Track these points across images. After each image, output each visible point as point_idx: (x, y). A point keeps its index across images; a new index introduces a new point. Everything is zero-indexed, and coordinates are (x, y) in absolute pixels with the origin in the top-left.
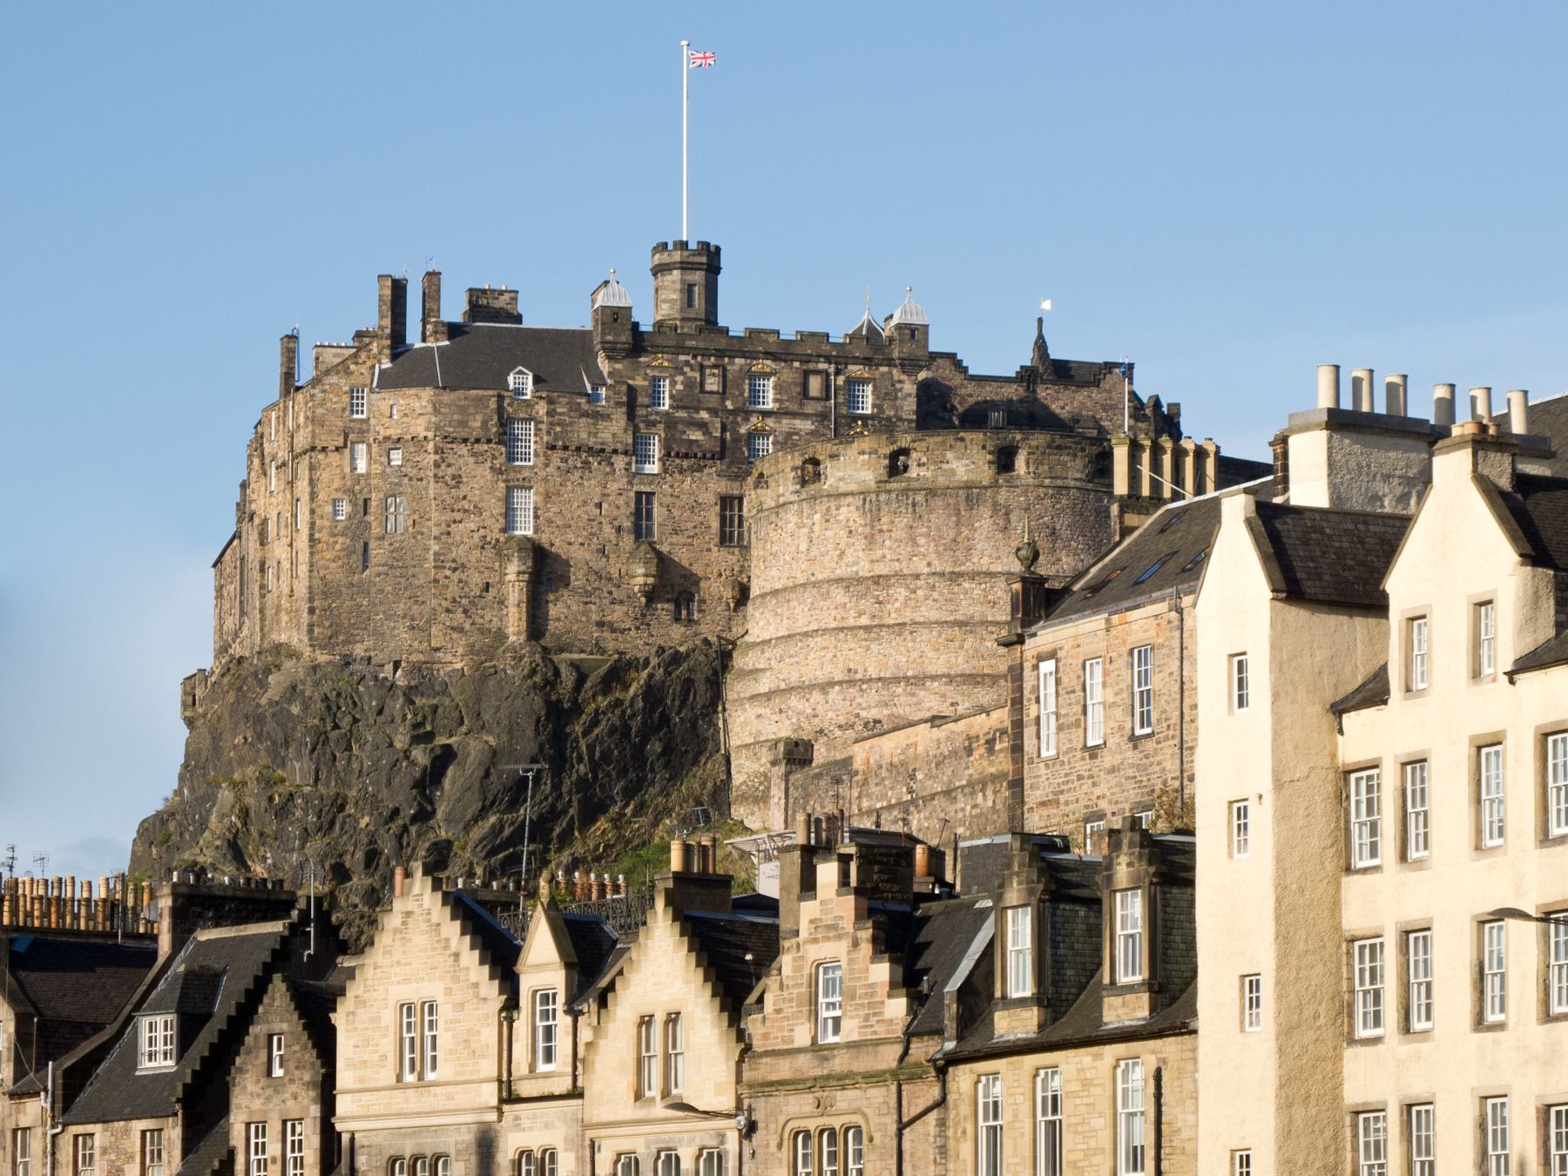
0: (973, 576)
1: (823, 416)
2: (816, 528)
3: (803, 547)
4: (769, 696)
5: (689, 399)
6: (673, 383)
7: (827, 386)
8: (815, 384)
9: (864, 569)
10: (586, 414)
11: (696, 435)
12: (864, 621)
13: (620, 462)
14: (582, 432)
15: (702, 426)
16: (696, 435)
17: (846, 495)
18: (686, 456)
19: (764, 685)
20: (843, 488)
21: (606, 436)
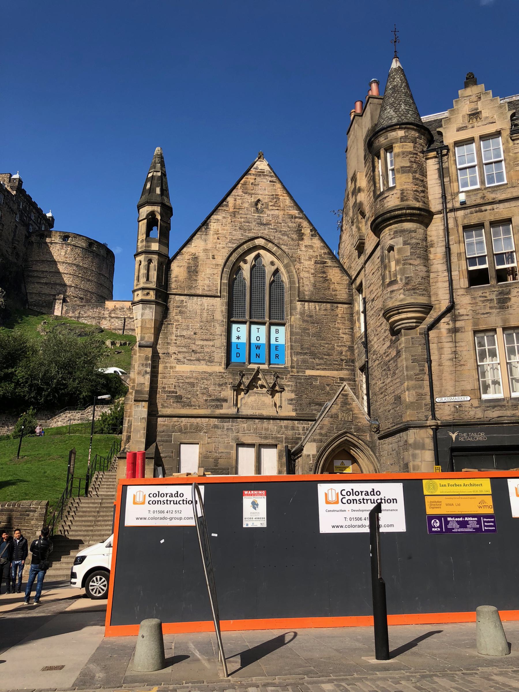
0: (103, 275)
1: (39, 228)
2: (68, 251)
3: (63, 254)
4: (46, 284)
5: (24, 208)
6: (23, 204)
7: (40, 222)
8: (39, 219)
9: (81, 264)
10: (12, 200)
11: (25, 218)
12: (80, 275)
13: (14, 215)
14: (11, 204)
15: (26, 217)
16: (25, 218)
17: (78, 247)
18: (23, 222)
19: (44, 281)
20: (77, 245)
21: (14, 208)
